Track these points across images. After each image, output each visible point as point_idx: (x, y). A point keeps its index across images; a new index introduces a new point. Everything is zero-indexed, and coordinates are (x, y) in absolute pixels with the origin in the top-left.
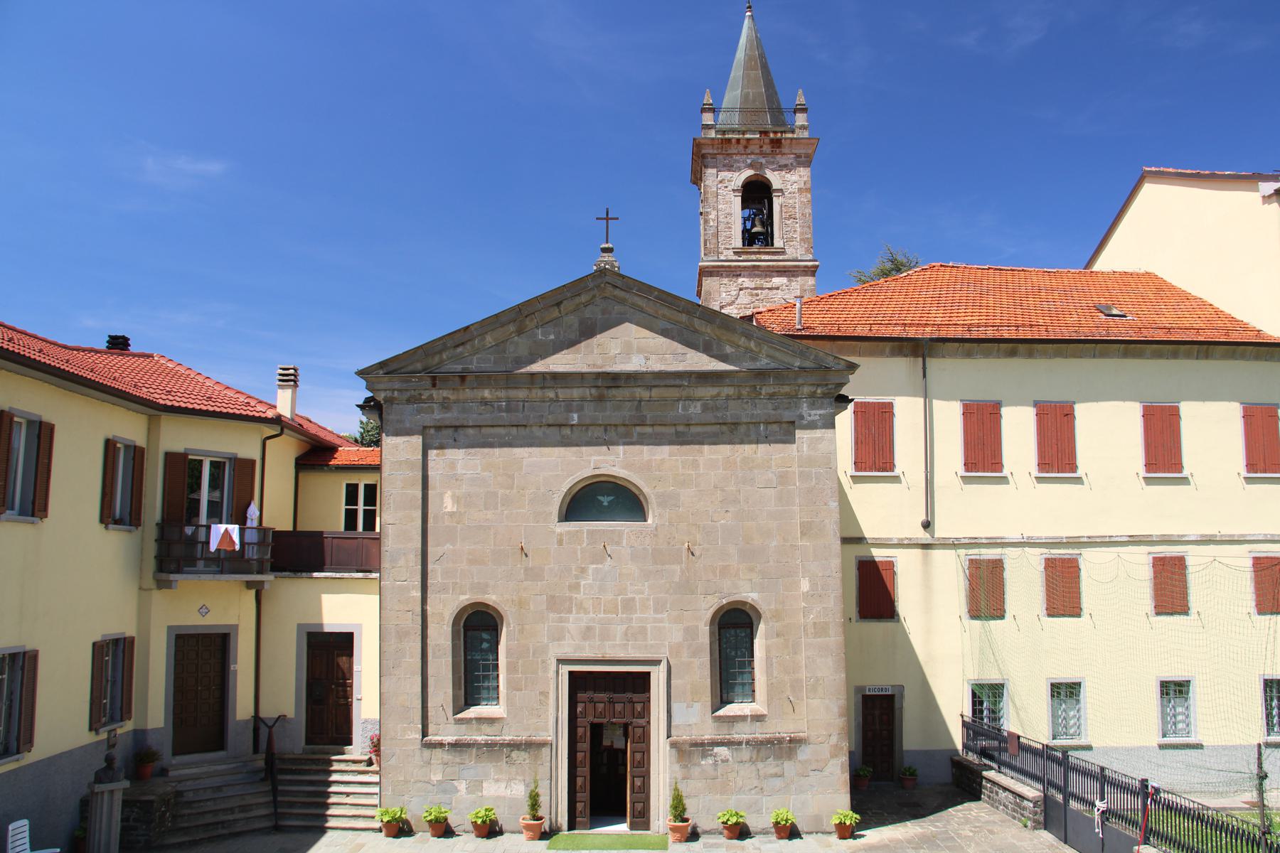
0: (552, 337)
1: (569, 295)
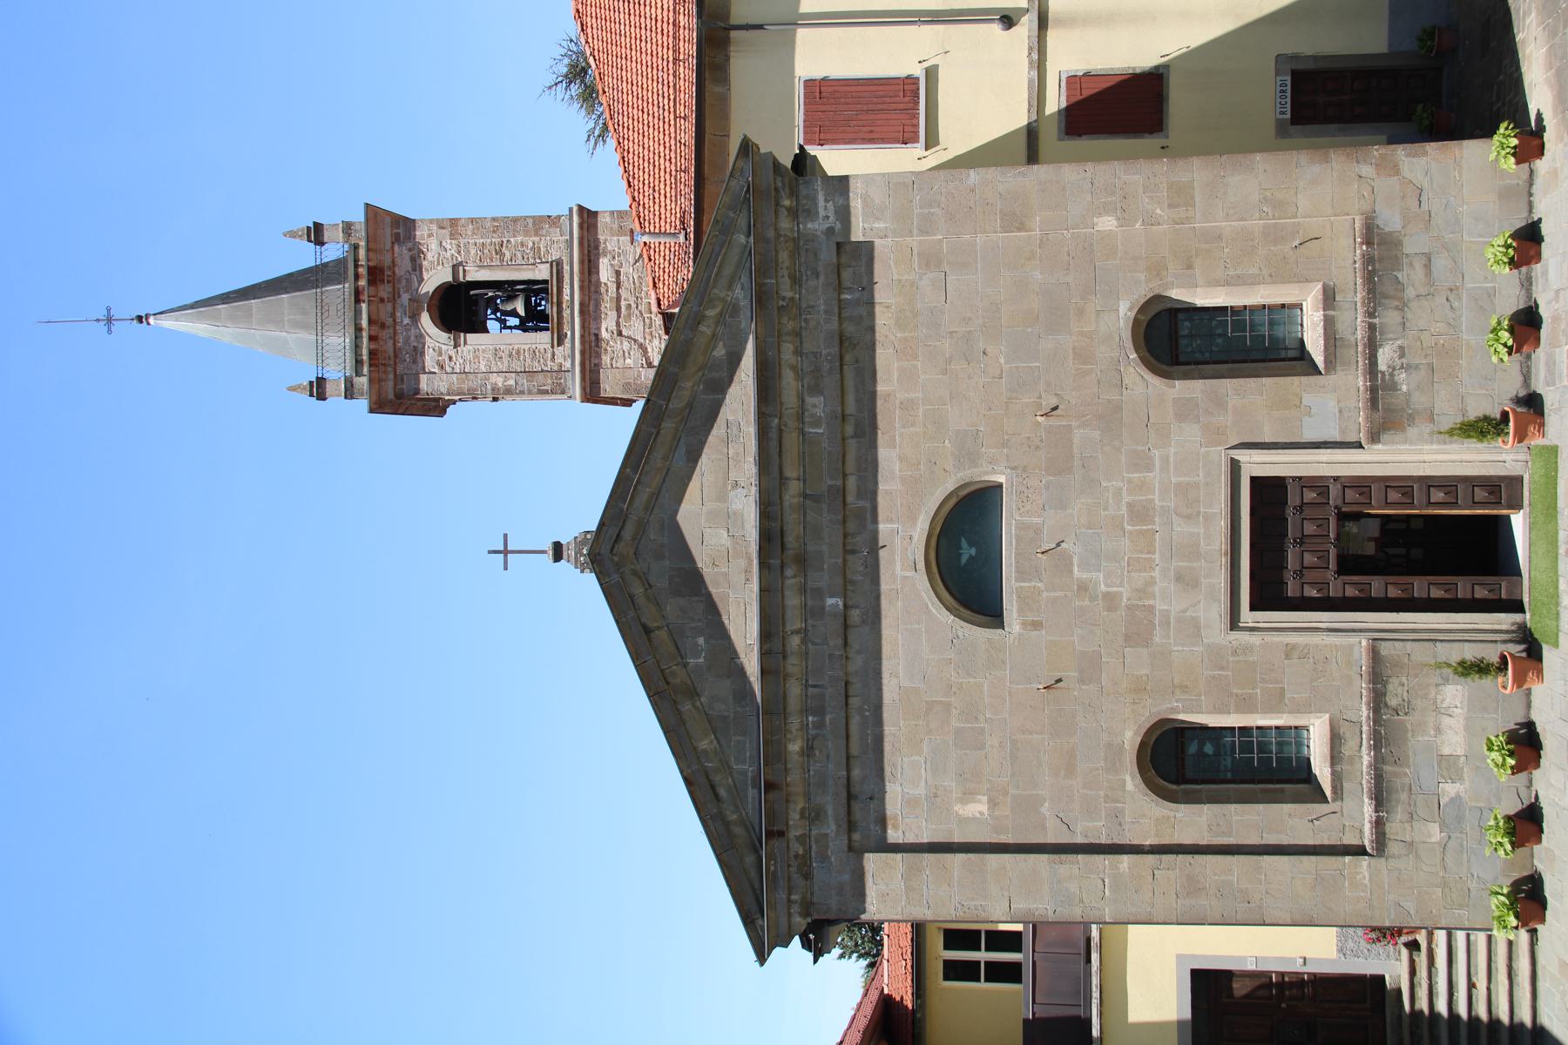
0: (701, 641)
1: (631, 614)
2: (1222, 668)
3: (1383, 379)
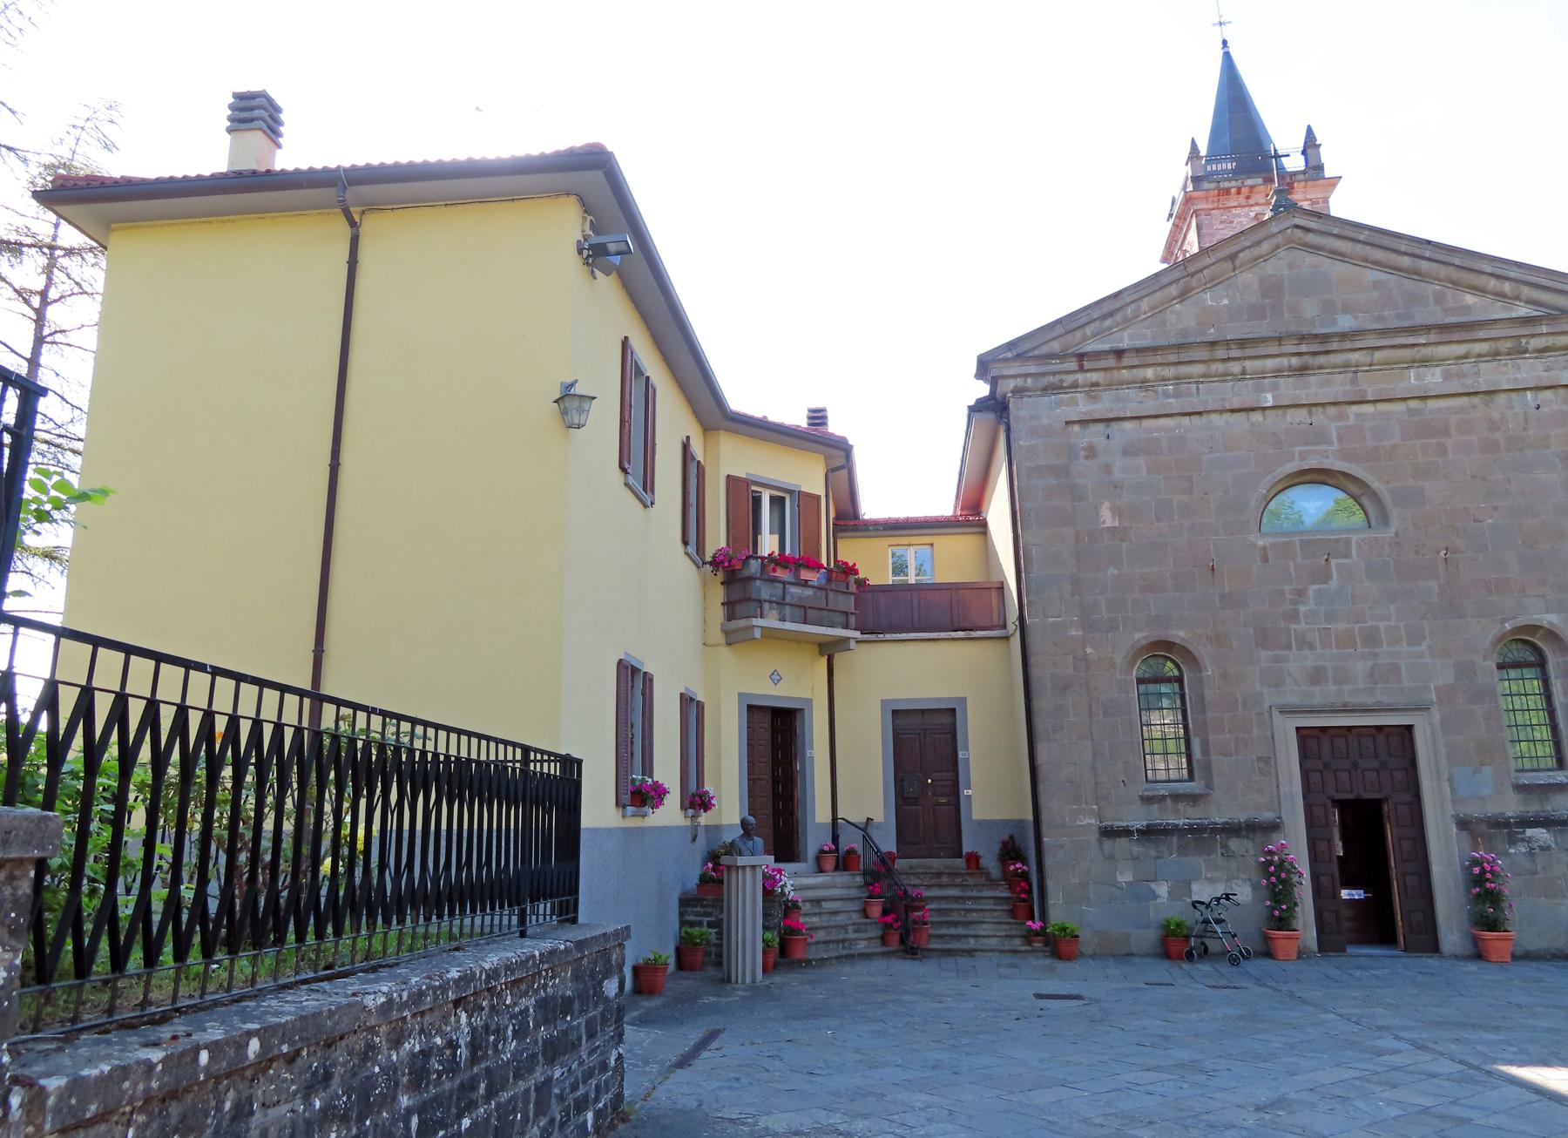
0: (1226, 302)
2: (1244, 705)
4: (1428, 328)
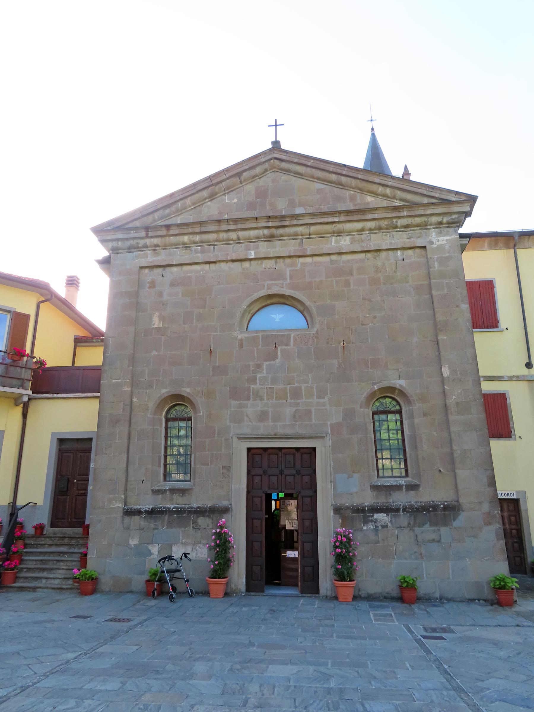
0: (235, 200)
2: (219, 434)
3: (369, 516)
4: (340, 213)
